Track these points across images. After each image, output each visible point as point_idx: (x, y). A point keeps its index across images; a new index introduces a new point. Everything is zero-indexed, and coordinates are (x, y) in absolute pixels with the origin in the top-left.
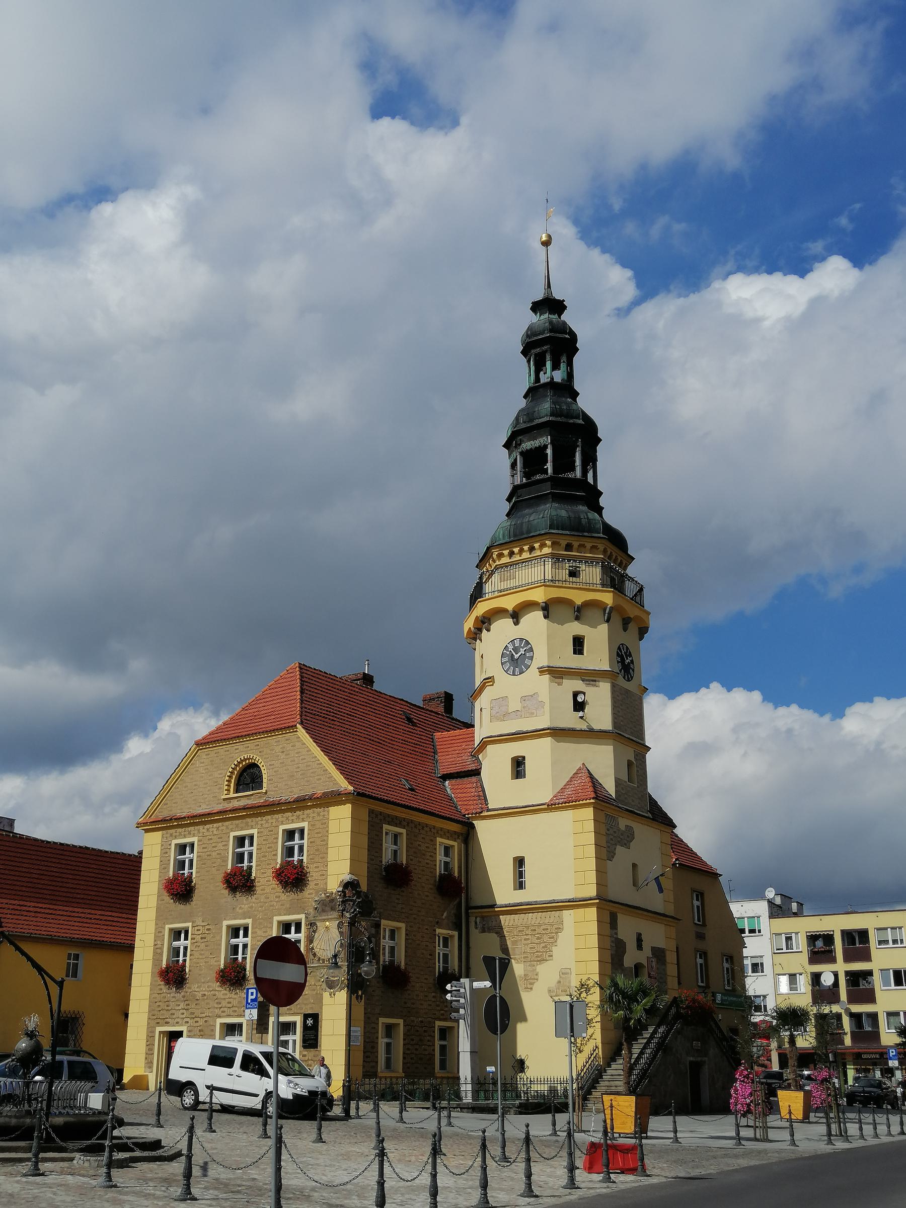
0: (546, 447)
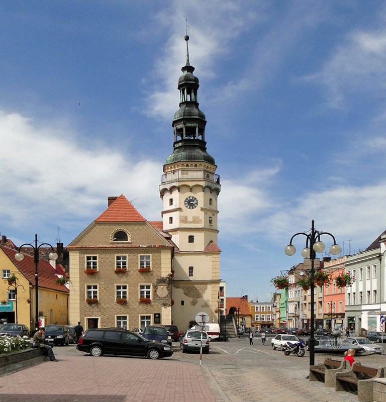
0: (196, 127)
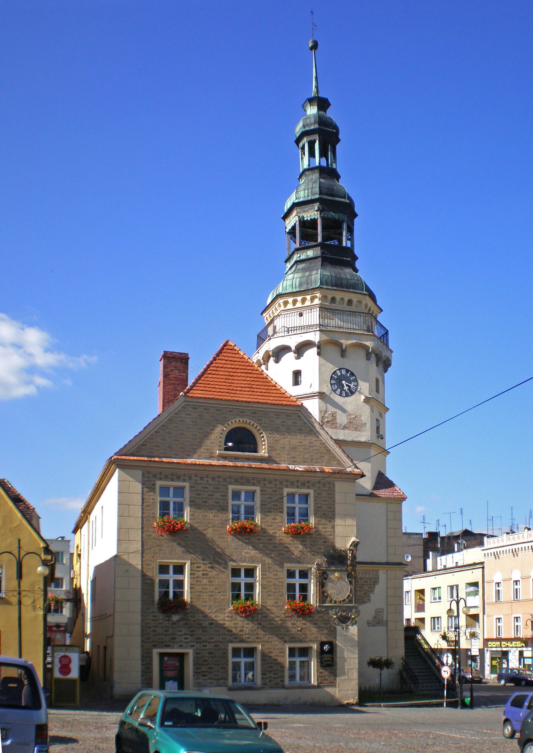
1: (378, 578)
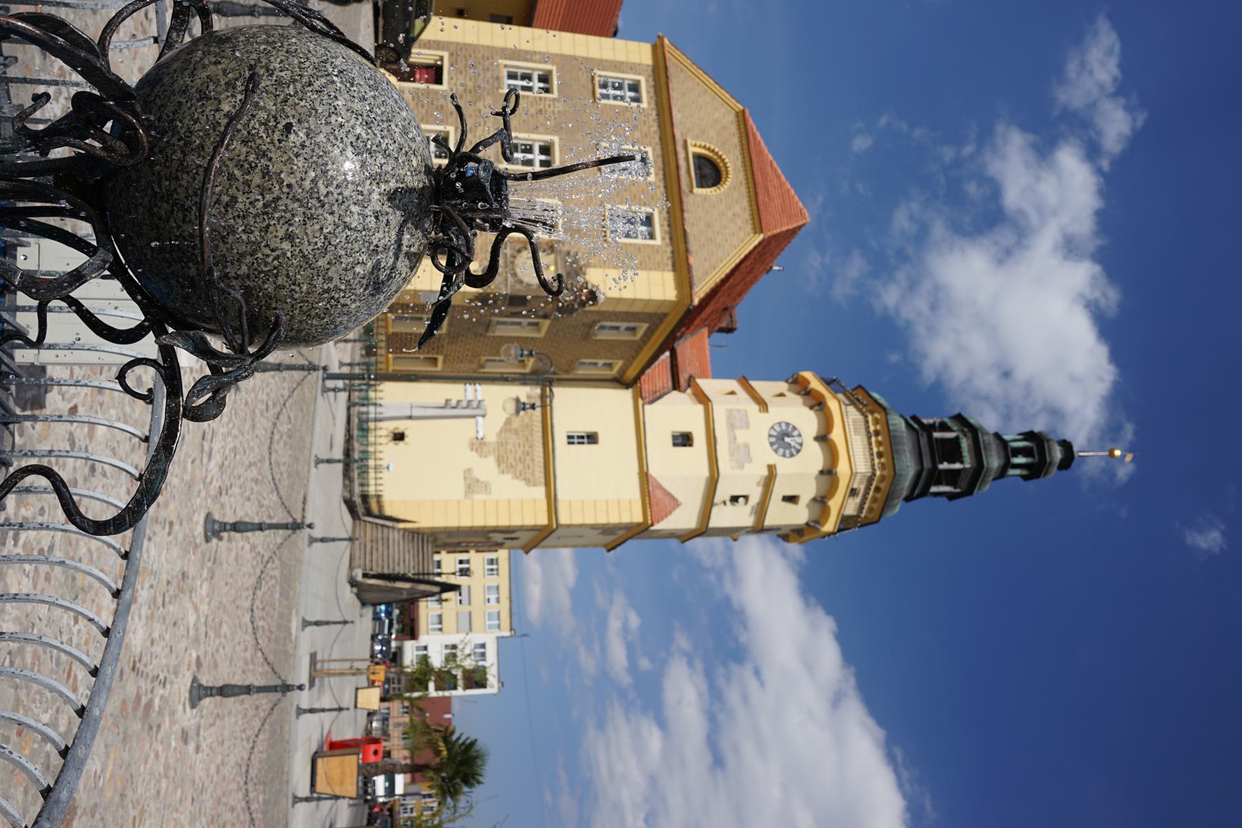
0: (962, 462)
1: (534, 485)
